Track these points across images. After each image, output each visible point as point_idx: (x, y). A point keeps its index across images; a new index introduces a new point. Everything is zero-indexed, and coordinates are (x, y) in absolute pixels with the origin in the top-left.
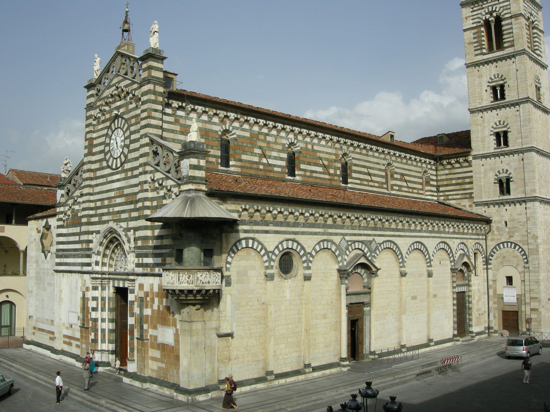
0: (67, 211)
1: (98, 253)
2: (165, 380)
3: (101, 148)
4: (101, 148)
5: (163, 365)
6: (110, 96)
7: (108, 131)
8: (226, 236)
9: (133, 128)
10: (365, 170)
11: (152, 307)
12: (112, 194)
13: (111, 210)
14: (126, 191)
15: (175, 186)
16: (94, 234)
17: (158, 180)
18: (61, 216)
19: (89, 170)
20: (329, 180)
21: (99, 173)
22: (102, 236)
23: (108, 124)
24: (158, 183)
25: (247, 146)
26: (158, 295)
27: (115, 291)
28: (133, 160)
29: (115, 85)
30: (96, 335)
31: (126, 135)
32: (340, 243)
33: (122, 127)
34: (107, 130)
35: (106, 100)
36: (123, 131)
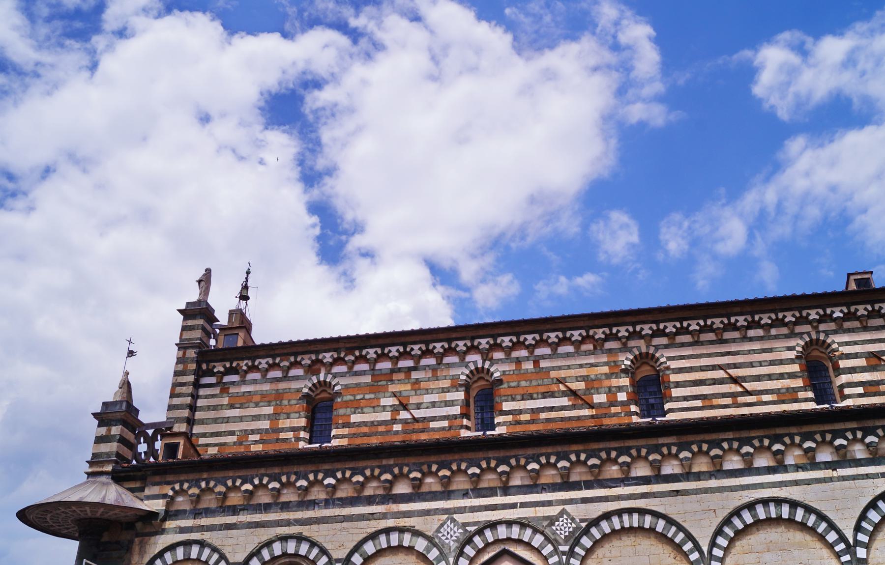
8: (141, 542)
10: (721, 374)
20: (592, 417)
25: (363, 399)
32: (438, 531)
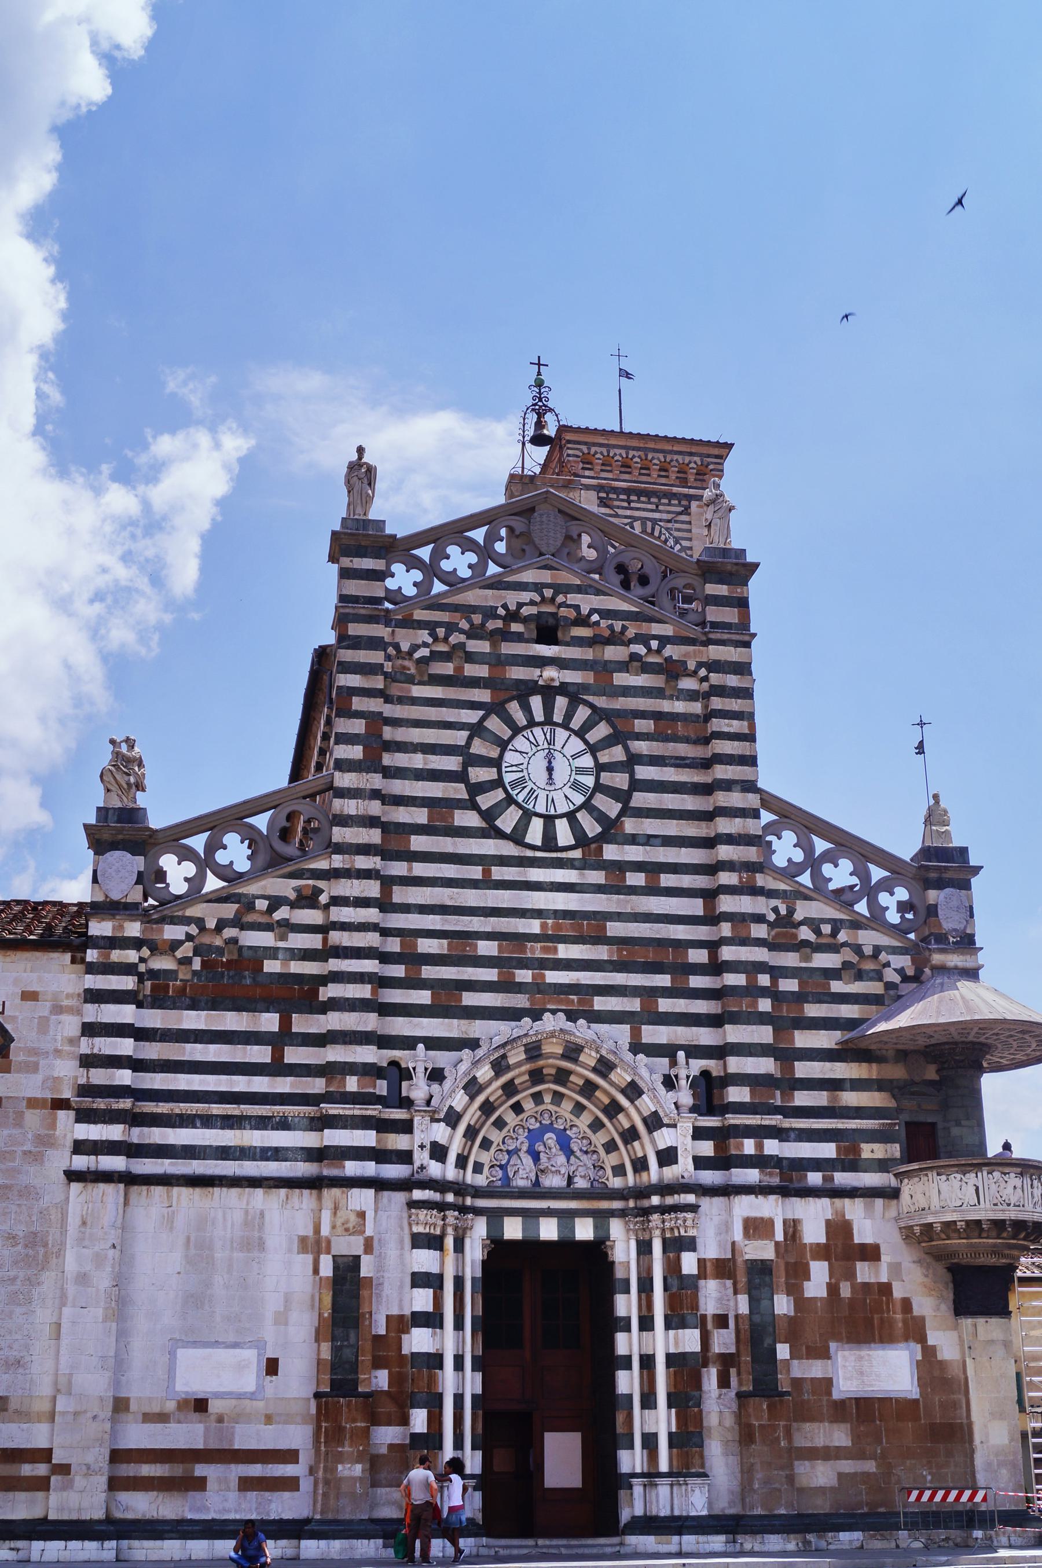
0: (180, 943)
1: (452, 1119)
2: (882, 1510)
3: (451, 763)
4: (451, 763)
5: (870, 1466)
6: (501, 612)
7: (483, 719)
9: (641, 747)
11: (794, 1290)
12: (534, 926)
13: (524, 976)
14: (614, 929)
15: (894, 951)
16: (421, 1046)
17: (814, 924)
18: (131, 956)
19: (371, 822)
21: (419, 843)
22: (496, 1055)
23: (483, 695)
24: (818, 932)
26: (822, 1252)
27: (486, 1257)
28: (659, 841)
29: (538, 587)
30: (435, 1420)
31: (604, 757)
33: (576, 723)
34: (481, 713)
35: (477, 619)
36: (586, 742)
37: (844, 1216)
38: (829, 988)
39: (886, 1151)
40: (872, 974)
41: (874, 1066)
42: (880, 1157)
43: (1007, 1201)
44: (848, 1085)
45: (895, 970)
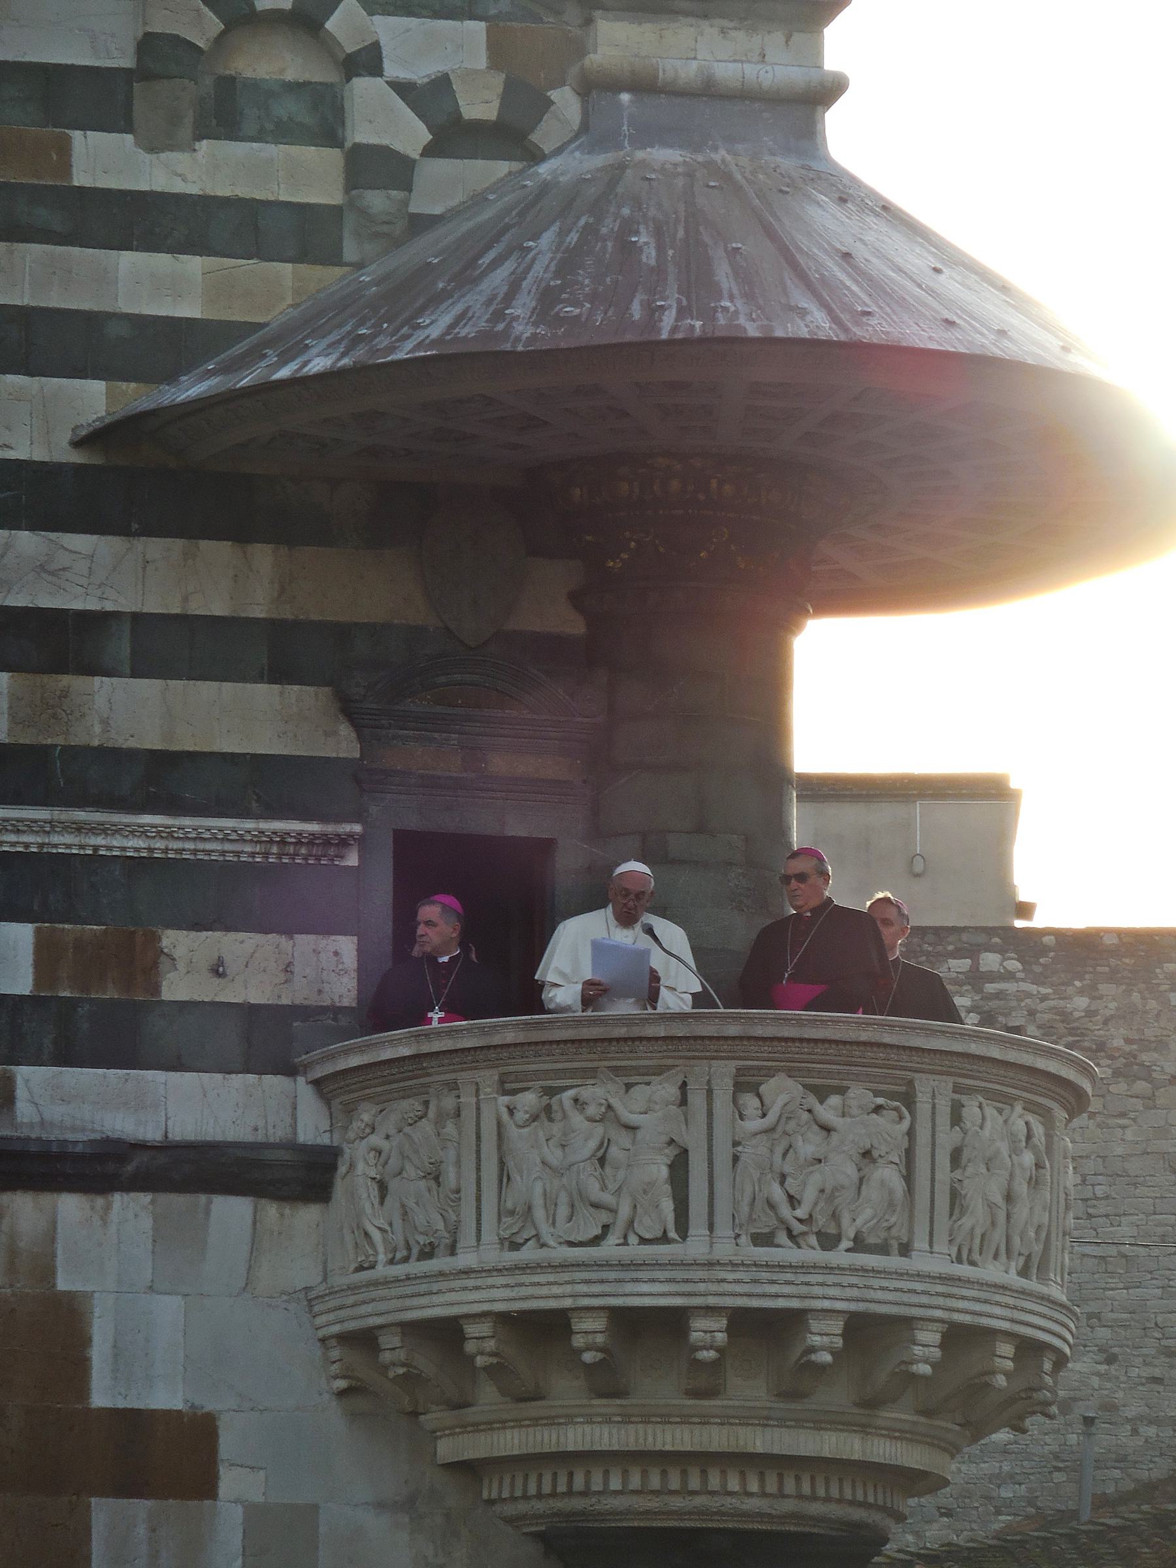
37: (47, 1273)
38: (65, 167)
39: (288, 969)
40: (288, 108)
41: (263, 556)
42: (257, 996)
43: (821, 1221)
44: (121, 647)
45: (403, 89)
